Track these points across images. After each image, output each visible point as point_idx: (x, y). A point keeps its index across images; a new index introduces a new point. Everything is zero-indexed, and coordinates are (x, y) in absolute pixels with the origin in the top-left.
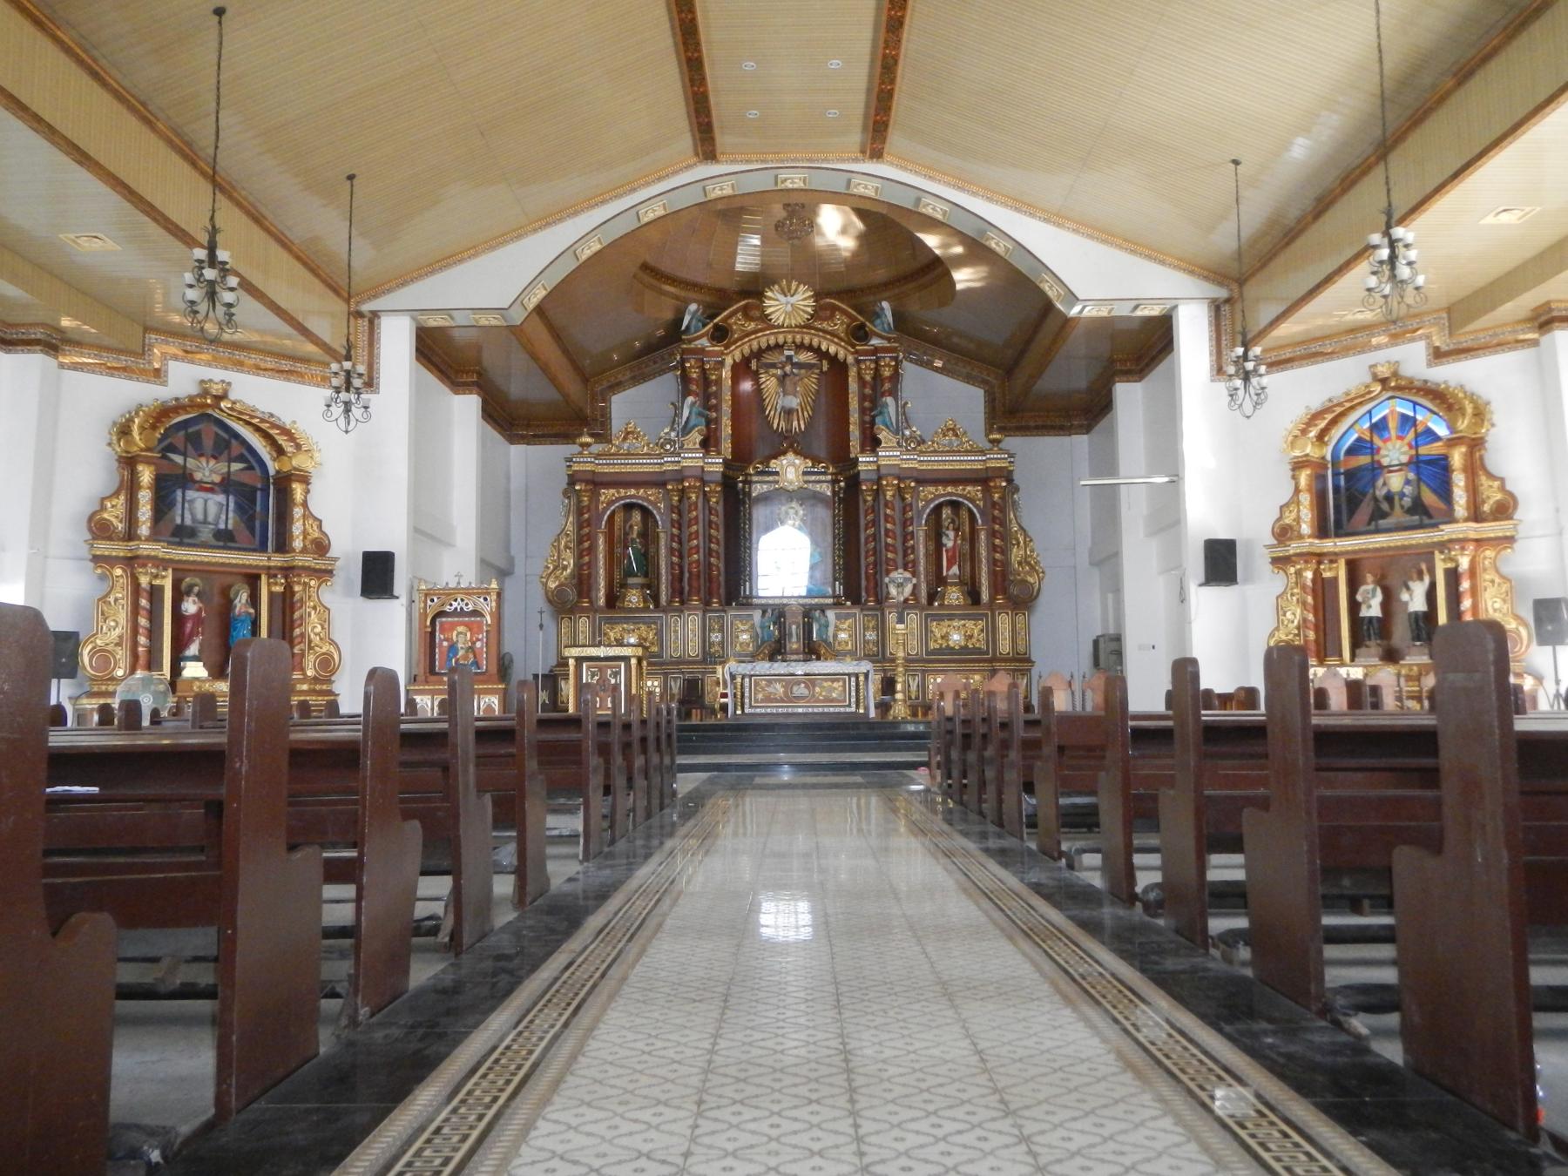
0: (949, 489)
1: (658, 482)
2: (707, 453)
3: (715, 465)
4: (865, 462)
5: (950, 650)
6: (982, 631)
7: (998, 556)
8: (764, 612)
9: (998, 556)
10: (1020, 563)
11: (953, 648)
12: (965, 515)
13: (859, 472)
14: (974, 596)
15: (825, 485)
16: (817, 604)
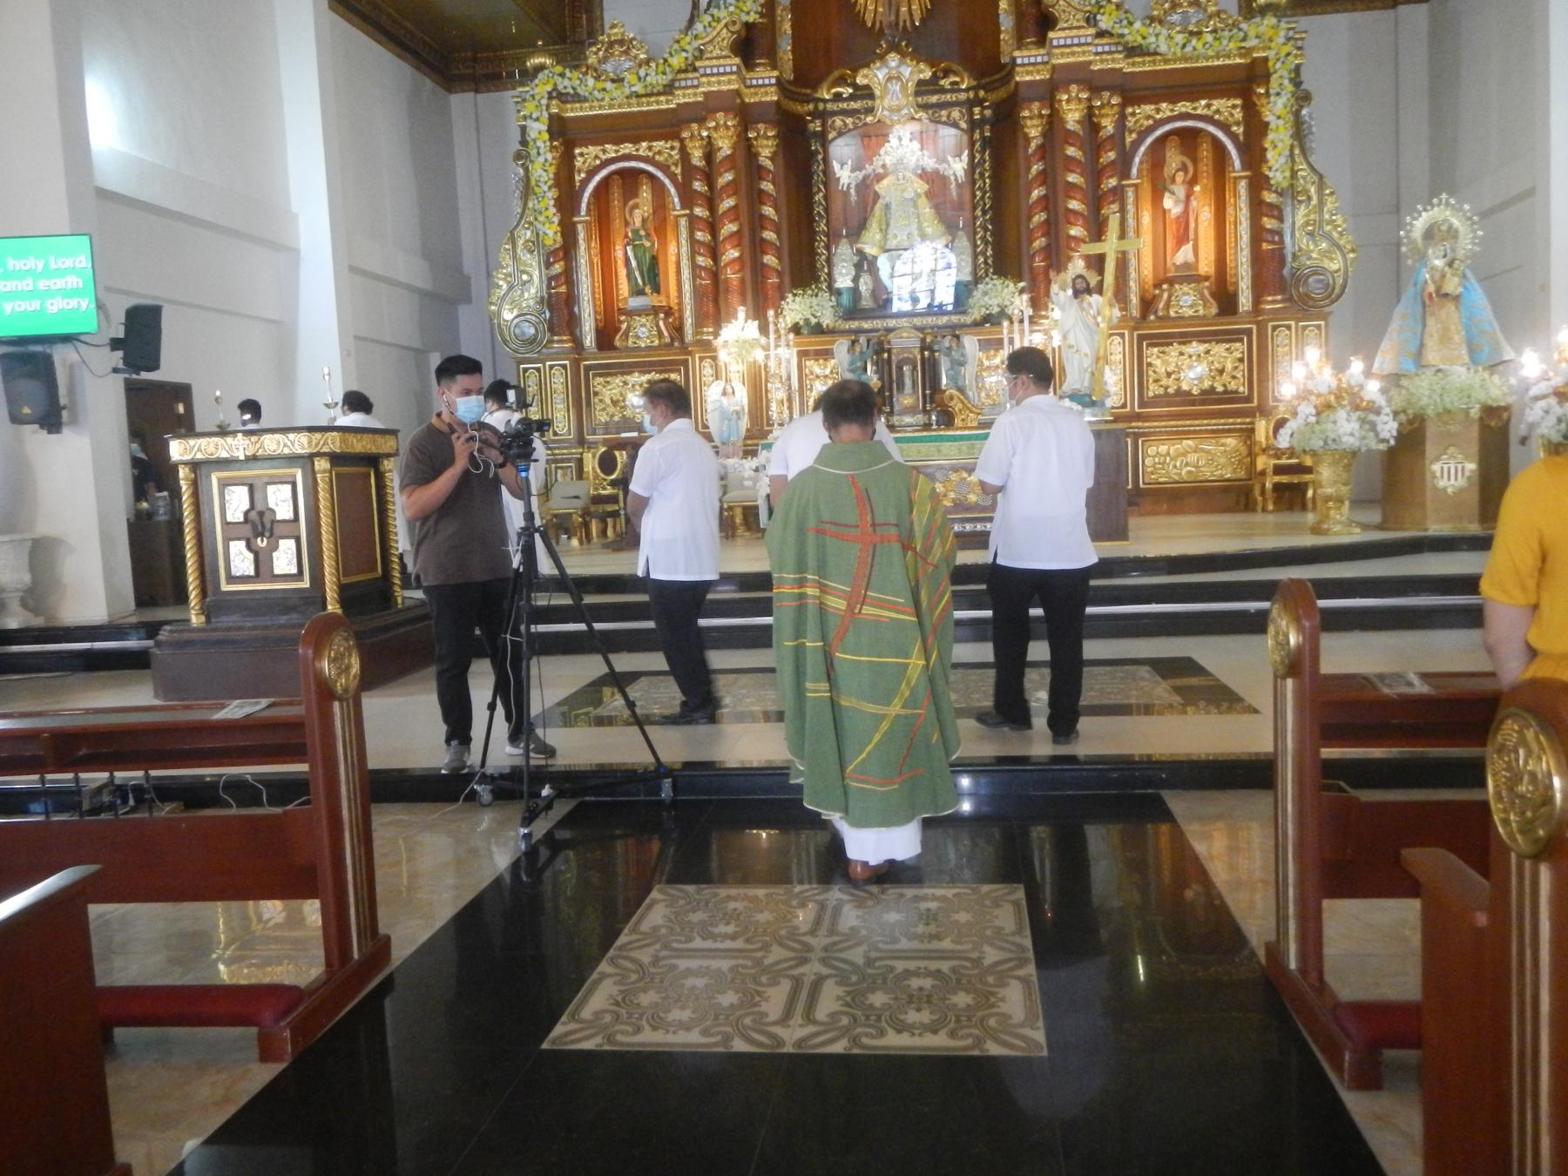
0: (1183, 107)
1: (669, 126)
2: (749, 63)
3: (763, 86)
4: (1029, 64)
5: (1183, 397)
6: (1241, 360)
7: (1269, 223)
8: (853, 342)
9: (1269, 223)
10: (1311, 234)
11: (1189, 393)
12: (1205, 152)
13: (1017, 84)
14: (1226, 301)
15: (956, 114)
16: (946, 327)
